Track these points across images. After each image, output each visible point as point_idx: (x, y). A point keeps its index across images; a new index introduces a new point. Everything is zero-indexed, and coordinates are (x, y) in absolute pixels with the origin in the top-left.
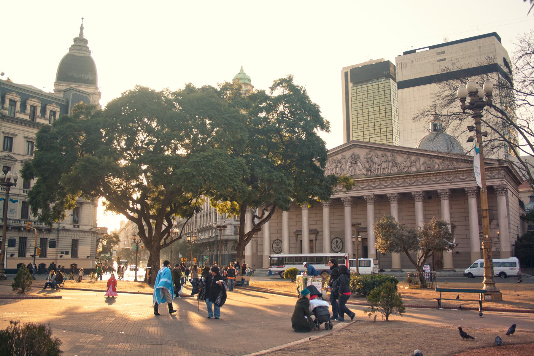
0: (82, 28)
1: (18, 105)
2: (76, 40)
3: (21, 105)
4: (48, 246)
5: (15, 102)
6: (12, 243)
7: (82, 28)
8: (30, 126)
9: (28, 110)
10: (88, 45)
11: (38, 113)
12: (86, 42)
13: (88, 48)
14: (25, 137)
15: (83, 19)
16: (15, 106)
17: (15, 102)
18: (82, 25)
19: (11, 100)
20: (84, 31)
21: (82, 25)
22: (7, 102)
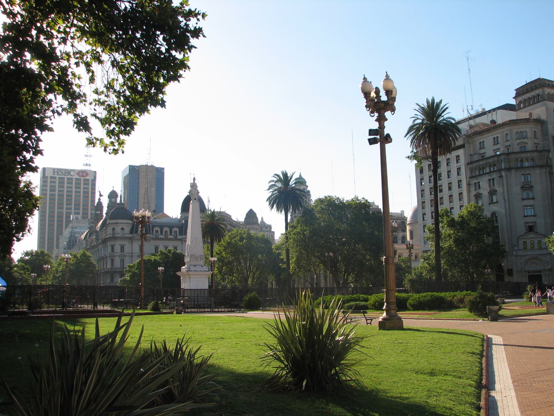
1: (159, 231)
3: (160, 231)
5: (158, 231)
8: (165, 240)
9: (164, 233)
11: (169, 234)
14: (164, 246)
16: (158, 232)
17: (158, 231)
19: (156, 230)
22: (154, 232)
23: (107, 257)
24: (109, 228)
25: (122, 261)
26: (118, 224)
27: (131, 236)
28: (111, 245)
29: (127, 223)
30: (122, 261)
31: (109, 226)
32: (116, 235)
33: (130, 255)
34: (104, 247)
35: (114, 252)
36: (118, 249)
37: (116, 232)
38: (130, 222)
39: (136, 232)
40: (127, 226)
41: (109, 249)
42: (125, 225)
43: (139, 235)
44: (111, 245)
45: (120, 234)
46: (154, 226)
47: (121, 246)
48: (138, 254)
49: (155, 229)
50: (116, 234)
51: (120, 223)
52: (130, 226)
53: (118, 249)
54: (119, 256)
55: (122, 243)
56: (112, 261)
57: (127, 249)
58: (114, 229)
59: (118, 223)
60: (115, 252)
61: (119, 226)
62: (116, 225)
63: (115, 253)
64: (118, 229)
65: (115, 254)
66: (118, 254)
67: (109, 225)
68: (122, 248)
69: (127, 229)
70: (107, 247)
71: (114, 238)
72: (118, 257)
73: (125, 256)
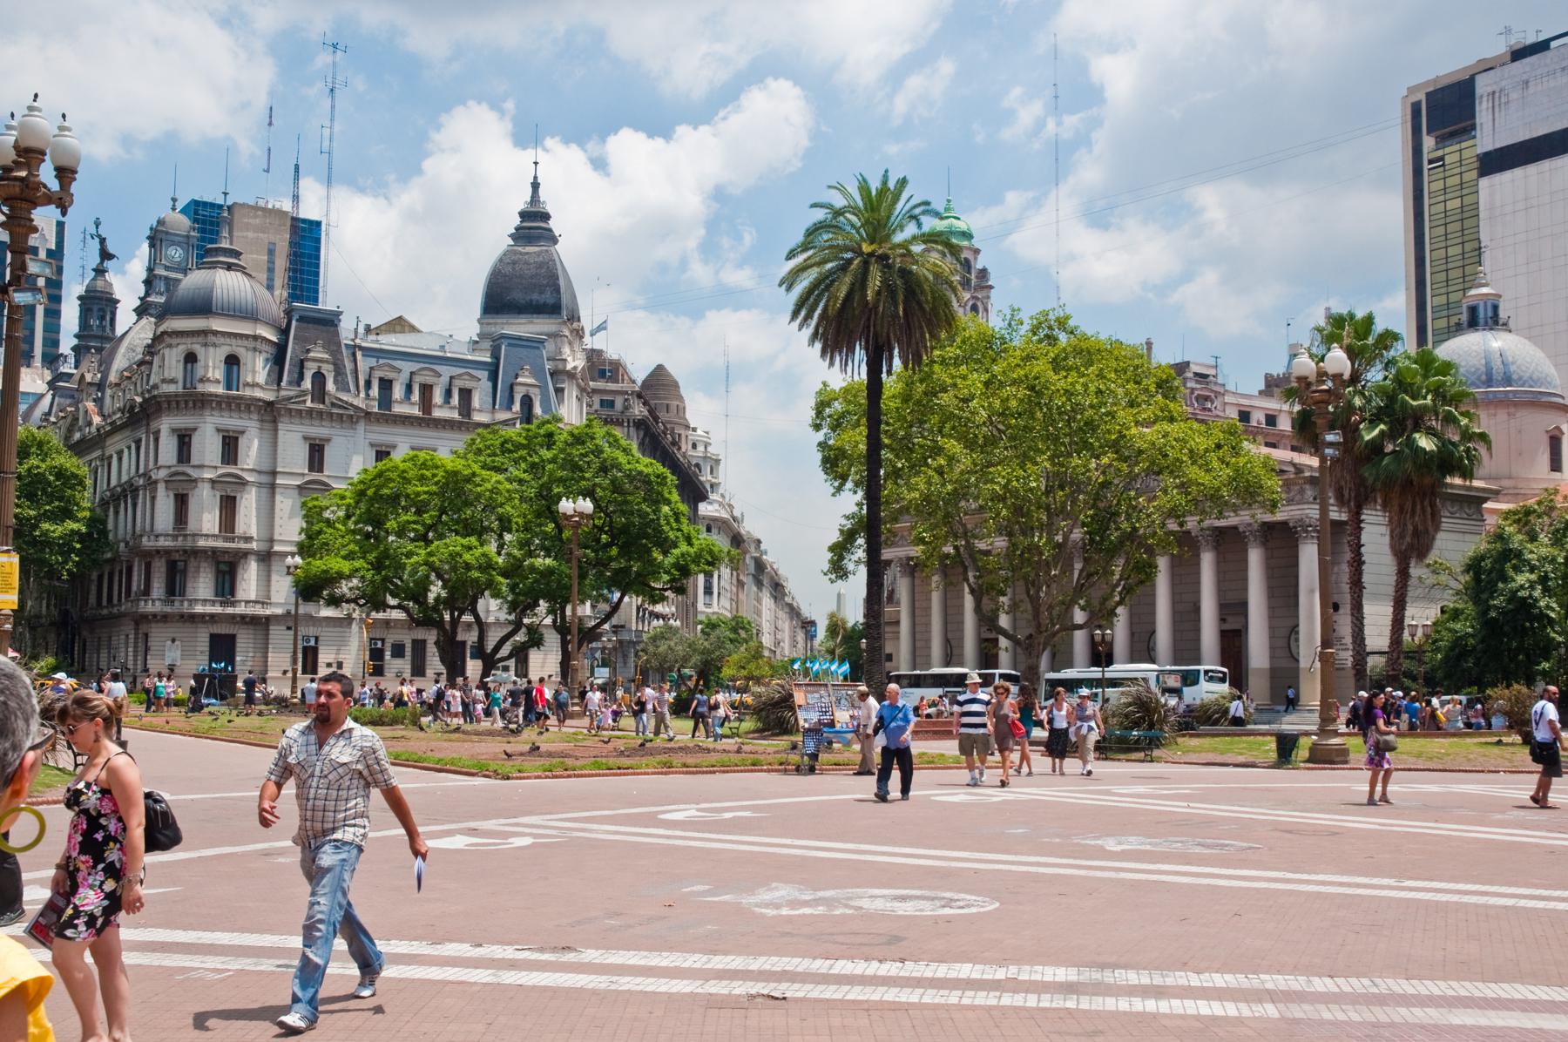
0: (535, 186)
2: (524, 215)
4: (468, 655)
6: (398, 651)
7: (535, 186)
10: (552, 224)
12: (546, 217)
13: (550, 230)
15: (536, 163)
18: (535, 178)
19: (381, 380)
20: (541, 191)
21: (535, 178)
23: (156, 482)
24: (167, 351)
26: (211, 339)
28: (174, 430)
29: (255, 338)
31: (170, 346)
32: (201, 388)
33: (265, 479)
34: (138, 442)
35: (188, 460)
37: (199, 372)
40: (255, 349)
41: (168, 449)
42: (246, 343)
44: (174, 430)
45: (218, 382)
47: (224, 438)
50: (201, 381)
51: (224, 334)
53: (207, 447)
55: (232, 422)
56: (181, 502)
57: (252, 452)
58: (191, 358)
59: (215, 333)
60: (195, 460)
61: (214, 345)
62: (201, 339)
63: (194, 467)
65: (194, 473)
66: (208, 475)
67: (168, 340)
70: (157, 440)
71: (197, 402)
72: (207, 486)
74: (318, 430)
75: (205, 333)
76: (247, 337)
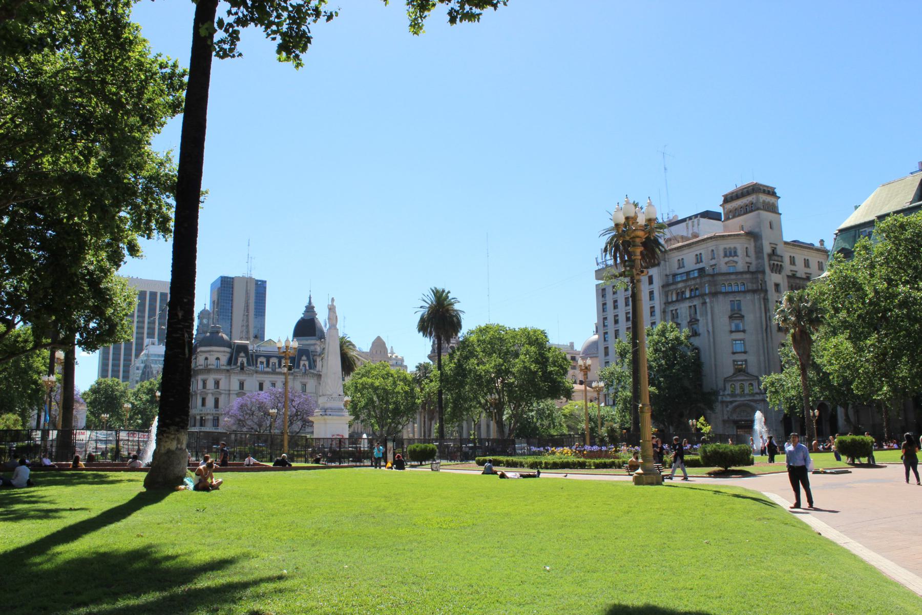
1: (265, 363)
5: (263, 362)
17: (263, 362)
19: (261, 362)
22: (259, 363)
25: (217, 401)
26: (212, 353)
27: (228, 368)
30: (217, 401)
32: (209, 367)
33: (227, 392)
36: (210, 384)
38: (228, 350)
39: (236, 363)
43: (238, 367)
46: (258, 356)
48: (236, 392)
49: (260, 360)
50: (210, 365)
51: (215, 351)
52: (228, 355)
53: (210, 384)
54: (212, 394)
55: (217, 376)
58: (206, 359)
59: (213, 351)
62: (209, 353)
64: (212, 359)
67: (200, 354)
68: (217, 383)
69: (224, 359)
71: (207, 370)
73: (221, 394)
74: (242, 377)
75: (210, 351)
76: (221, 352)
